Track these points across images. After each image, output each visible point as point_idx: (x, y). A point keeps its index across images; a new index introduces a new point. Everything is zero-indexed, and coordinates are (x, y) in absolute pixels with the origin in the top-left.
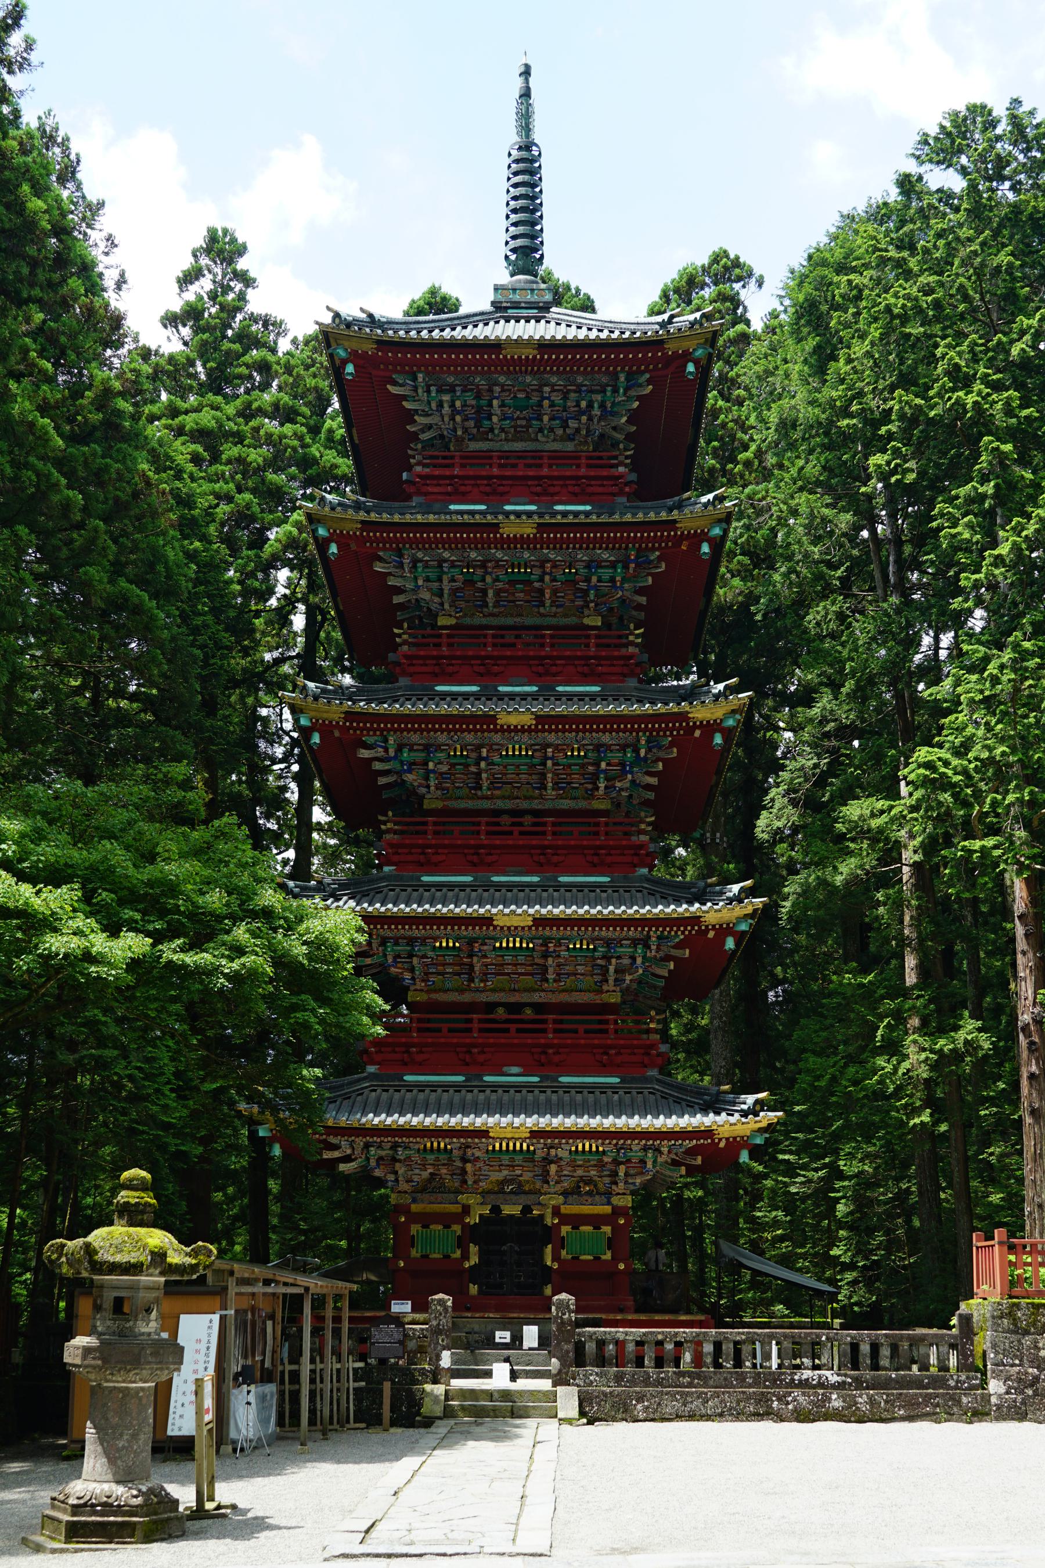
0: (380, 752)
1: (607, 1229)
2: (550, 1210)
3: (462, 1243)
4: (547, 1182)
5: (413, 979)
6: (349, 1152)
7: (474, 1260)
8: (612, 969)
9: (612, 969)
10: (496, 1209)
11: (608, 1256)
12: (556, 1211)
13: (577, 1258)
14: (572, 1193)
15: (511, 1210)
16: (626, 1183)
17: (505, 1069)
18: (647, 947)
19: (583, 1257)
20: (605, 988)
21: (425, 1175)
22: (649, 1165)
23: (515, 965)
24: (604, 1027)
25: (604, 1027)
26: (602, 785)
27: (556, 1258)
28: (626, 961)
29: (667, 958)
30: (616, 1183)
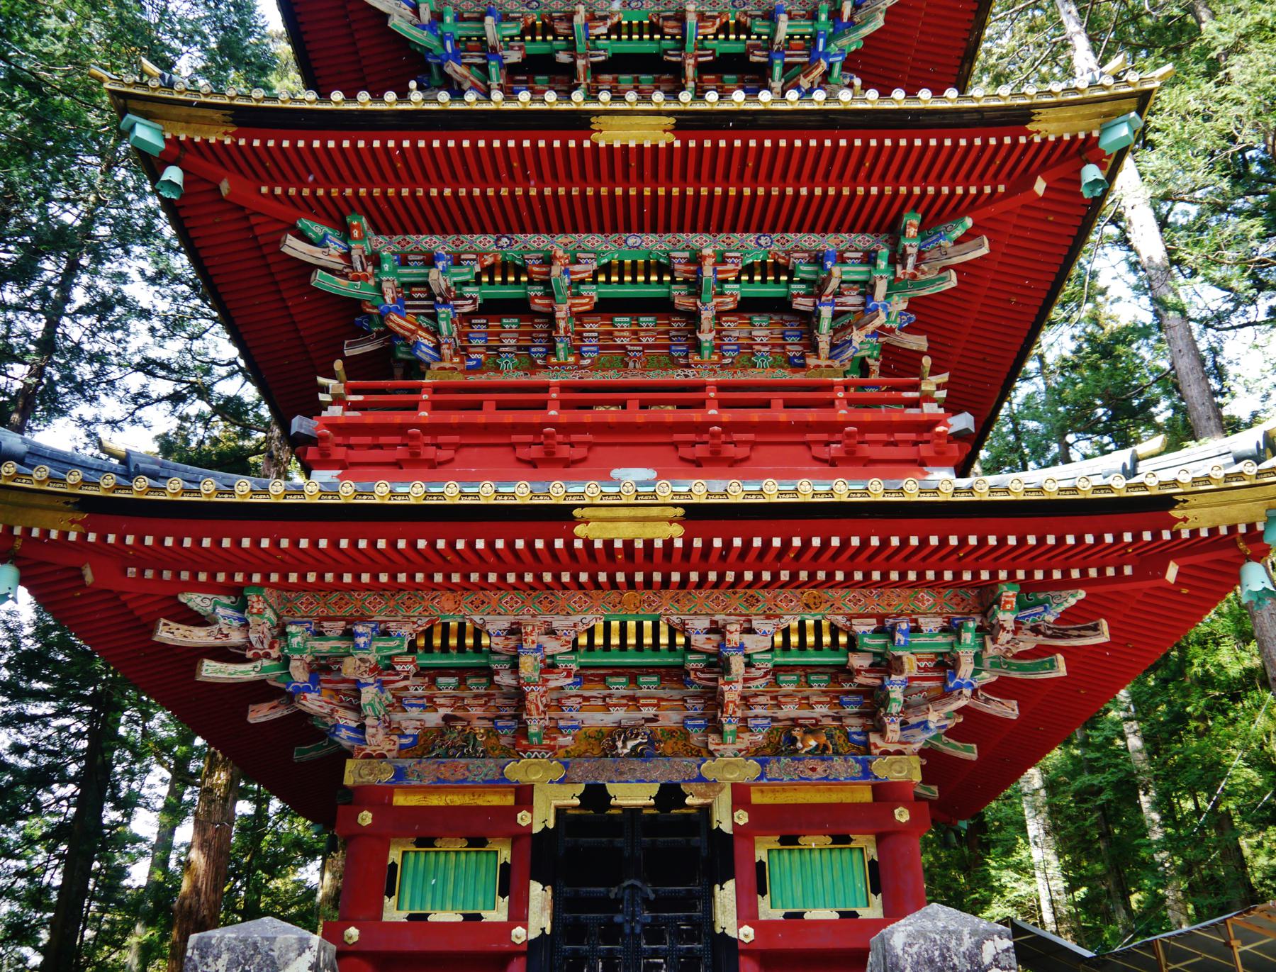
3: (510, 885)
4: (719, 731)
5: (437, 348)
6: (236, 638)
8: (826, 312)
9: (826, 312)
10: (596, 796)
12: (740, 796)
13: (800, 915)
14: (777, 753)
15: (632, 794)
17: (616, 473)
18: (897, 258)
20: (812, 361)
21: (433, 719)
22: (966, 669)
24: (827, 395)
25: (827, 395)
27: (746, 914)
28: (852, 300)
30: (881, 730)
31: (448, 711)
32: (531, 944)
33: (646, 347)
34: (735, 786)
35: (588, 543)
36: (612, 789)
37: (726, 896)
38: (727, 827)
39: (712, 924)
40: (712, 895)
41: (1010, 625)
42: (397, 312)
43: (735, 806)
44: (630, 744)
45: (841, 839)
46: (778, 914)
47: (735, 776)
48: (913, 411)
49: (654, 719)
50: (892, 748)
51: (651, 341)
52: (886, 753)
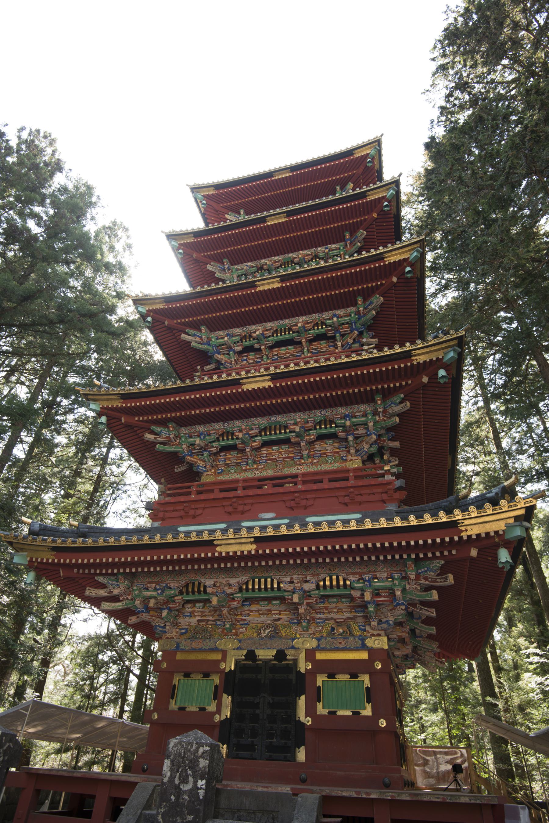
0: (198, 339)
1: (366, 679)
2: (302, 656)
5: (205, 467)
7: (227, 712)
11: (367, 711)
12: (310, 655)
13: (335, 712)
15: (266, 654)
16: (380, 622)
17: (261, 516)
19: (340, 713)
23: (280, 452)
25: (346, 475)
26: (339, 344)
27: (310, 711)
29: (392, 415)
31: (199, 618)
32: (222, 722)
33: (285, 458)
34: (307, 650)
35: (221, 553)
36: (257, 652)
37: (302, 701)
38: (303, 670)
39: (295, 715)
40: (296, 702)
41: (413, 577)
42: (190, 456)
43: (307, 660)
44: (267, 632)
45: (354, 676)
46: (325, 712)
47: (308, 646)
48: (380, 479)
49: (279, 619)
50: (375, 633)
51: (286, 455)
52: (373, 635)
